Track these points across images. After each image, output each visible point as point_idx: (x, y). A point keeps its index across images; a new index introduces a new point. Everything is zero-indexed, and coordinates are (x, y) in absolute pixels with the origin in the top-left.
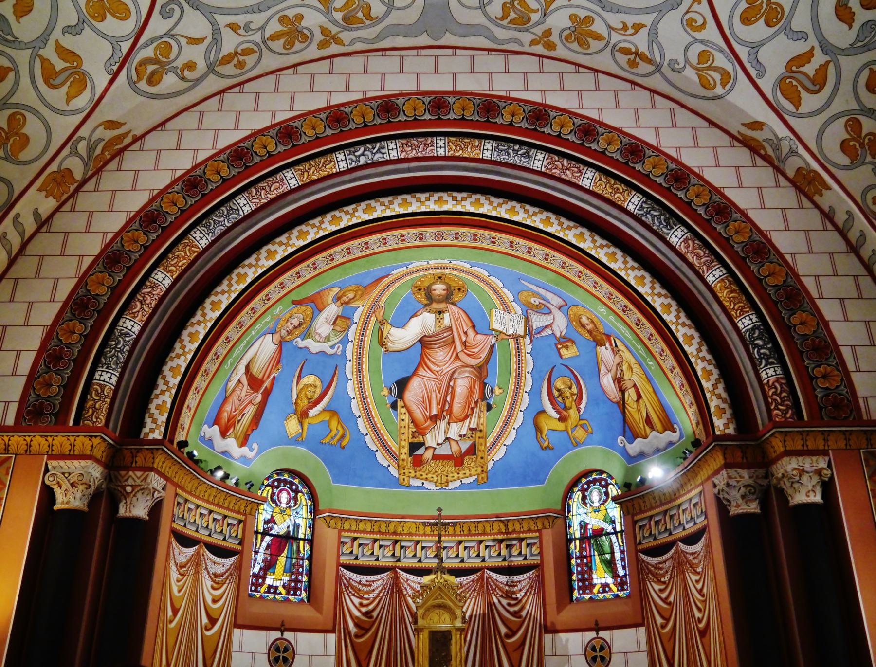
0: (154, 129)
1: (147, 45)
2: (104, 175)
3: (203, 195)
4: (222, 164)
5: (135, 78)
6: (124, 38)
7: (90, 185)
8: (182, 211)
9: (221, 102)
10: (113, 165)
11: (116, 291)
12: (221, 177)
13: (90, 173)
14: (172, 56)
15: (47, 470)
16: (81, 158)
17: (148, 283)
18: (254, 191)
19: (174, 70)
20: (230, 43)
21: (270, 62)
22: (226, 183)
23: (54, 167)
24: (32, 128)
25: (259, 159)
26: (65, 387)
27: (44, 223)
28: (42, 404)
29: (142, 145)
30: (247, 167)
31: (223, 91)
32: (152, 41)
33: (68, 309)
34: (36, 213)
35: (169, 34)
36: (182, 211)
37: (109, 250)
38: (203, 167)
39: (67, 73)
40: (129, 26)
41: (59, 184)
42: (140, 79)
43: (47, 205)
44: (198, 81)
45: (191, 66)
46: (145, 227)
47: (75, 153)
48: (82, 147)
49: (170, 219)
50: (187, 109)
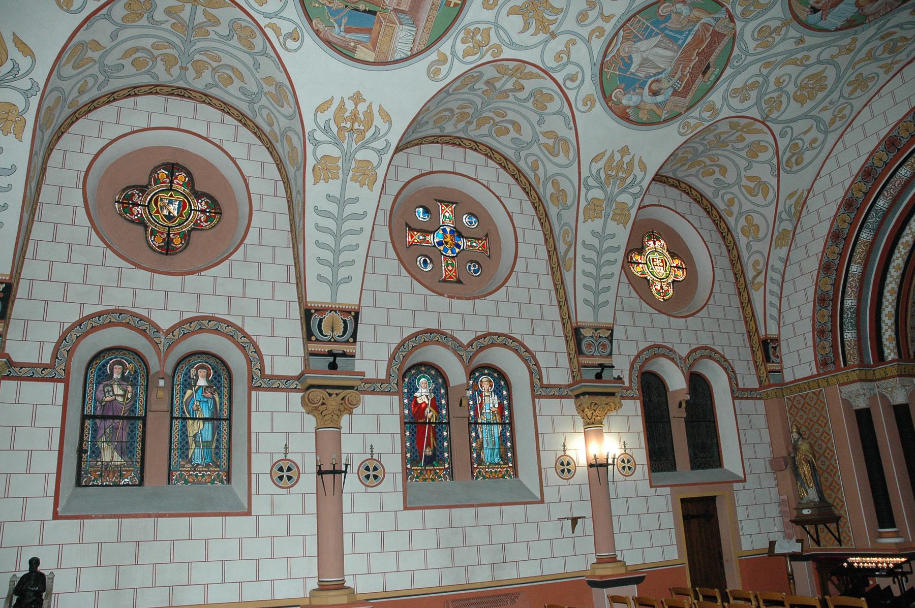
0: (815, 180)
1: (784, 153)
2: (802, 219)
3: (858, 209)
4: (860, 184)
5: (788, 169)
6: (772, 158)
7: (799, 230)
8: (851, 224)
9: (844, 143)
10: (804, 212)
11: (835, 285)
12: (863, 192)
13: (795, 223)
14: (801, 146)
15: (841, 392)
16: (786, 220)
17: (849, 275)
18: (885, 192)
19: (807, 149)
20: (827, 116)
21: (858, 104)
22: (867, 195)
23: (776, 234)
24: (757, 219)
25: (881, 169)
26: (832, 346)
27: (786, 261)
28: (825, 359)
29: (814, 193)
30: (875, 179)
31: (842, 135)
32: (786, 149)
33: (817, 304)
34: (780, 258)
35: (791, 140)
36: (851, 224)
37: (823, 263)
38: (850, 191)
39: (757, 187)
40: (771, 152)
41: (783, 239)
42: (791, 168)
43: (783, 252)
44: (823, 142)
45: (814, 140)
46: (835, 242)
47: (782, 220)
48: (784, 216)
49: (846, 231)
50: (827, 158)
